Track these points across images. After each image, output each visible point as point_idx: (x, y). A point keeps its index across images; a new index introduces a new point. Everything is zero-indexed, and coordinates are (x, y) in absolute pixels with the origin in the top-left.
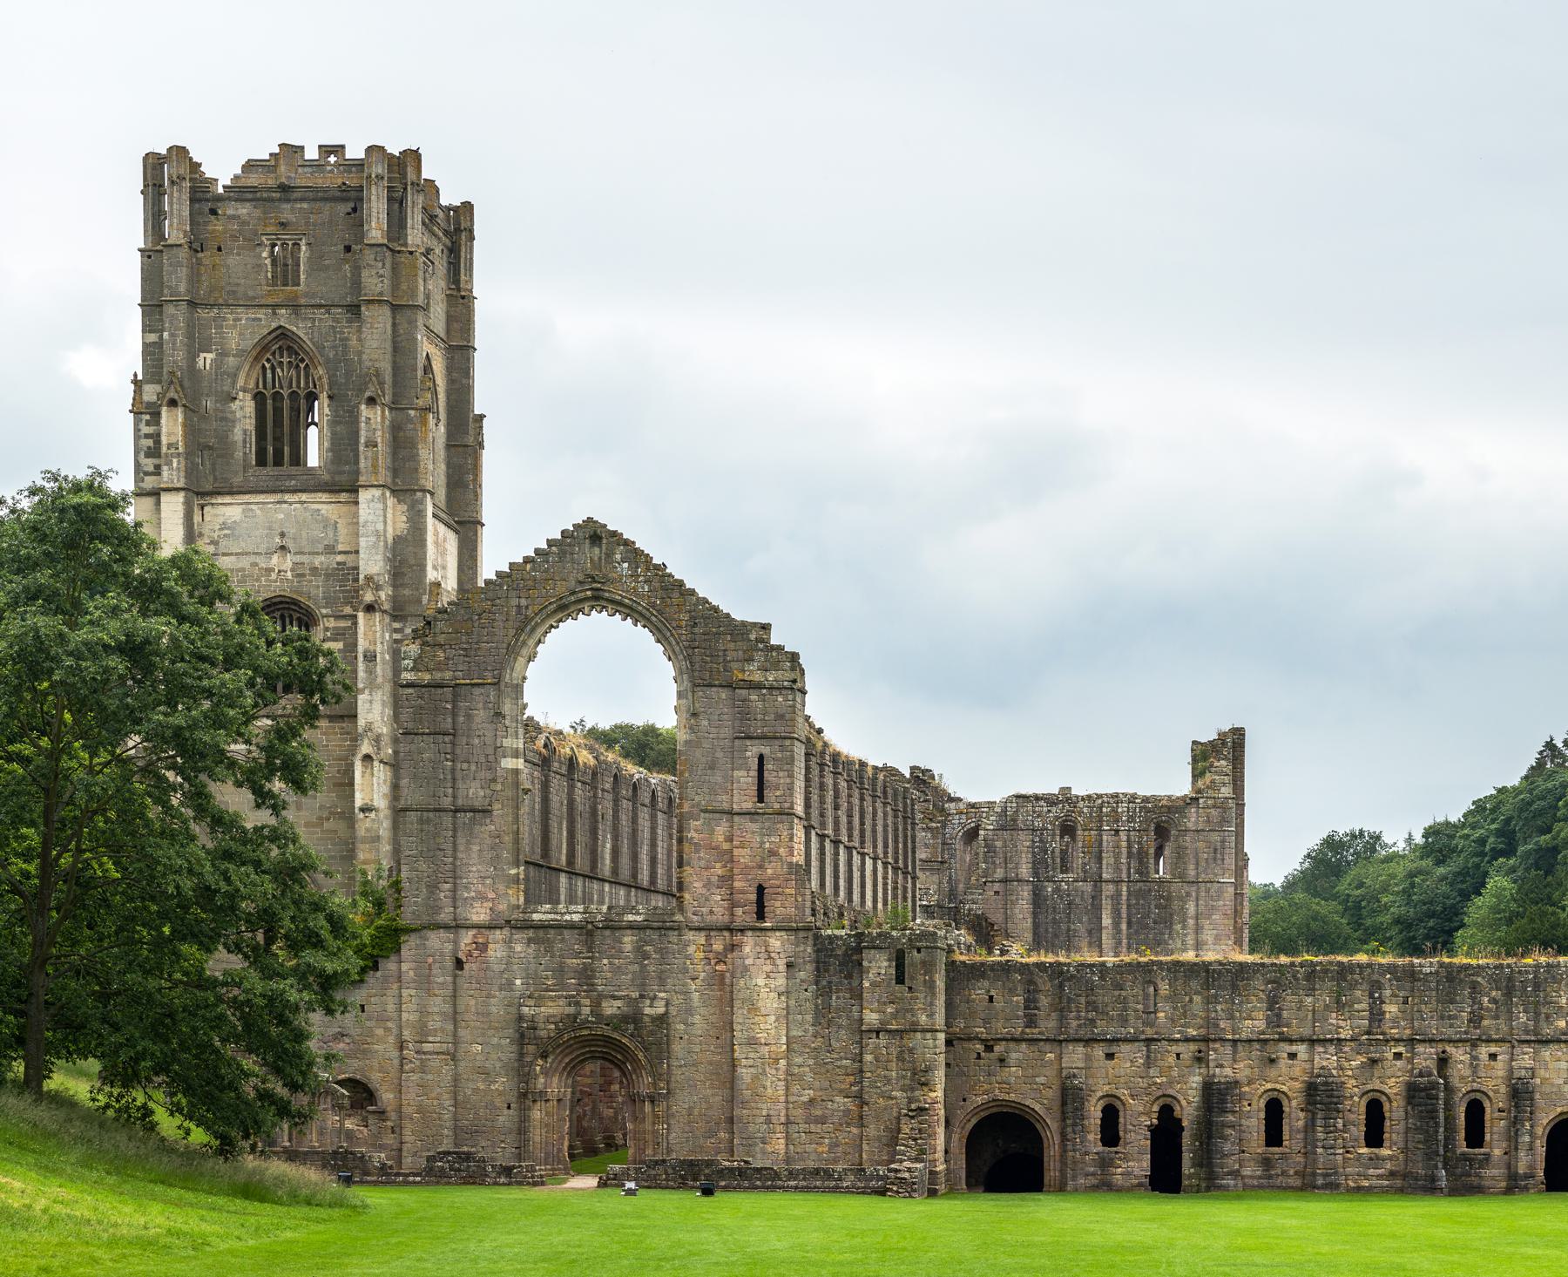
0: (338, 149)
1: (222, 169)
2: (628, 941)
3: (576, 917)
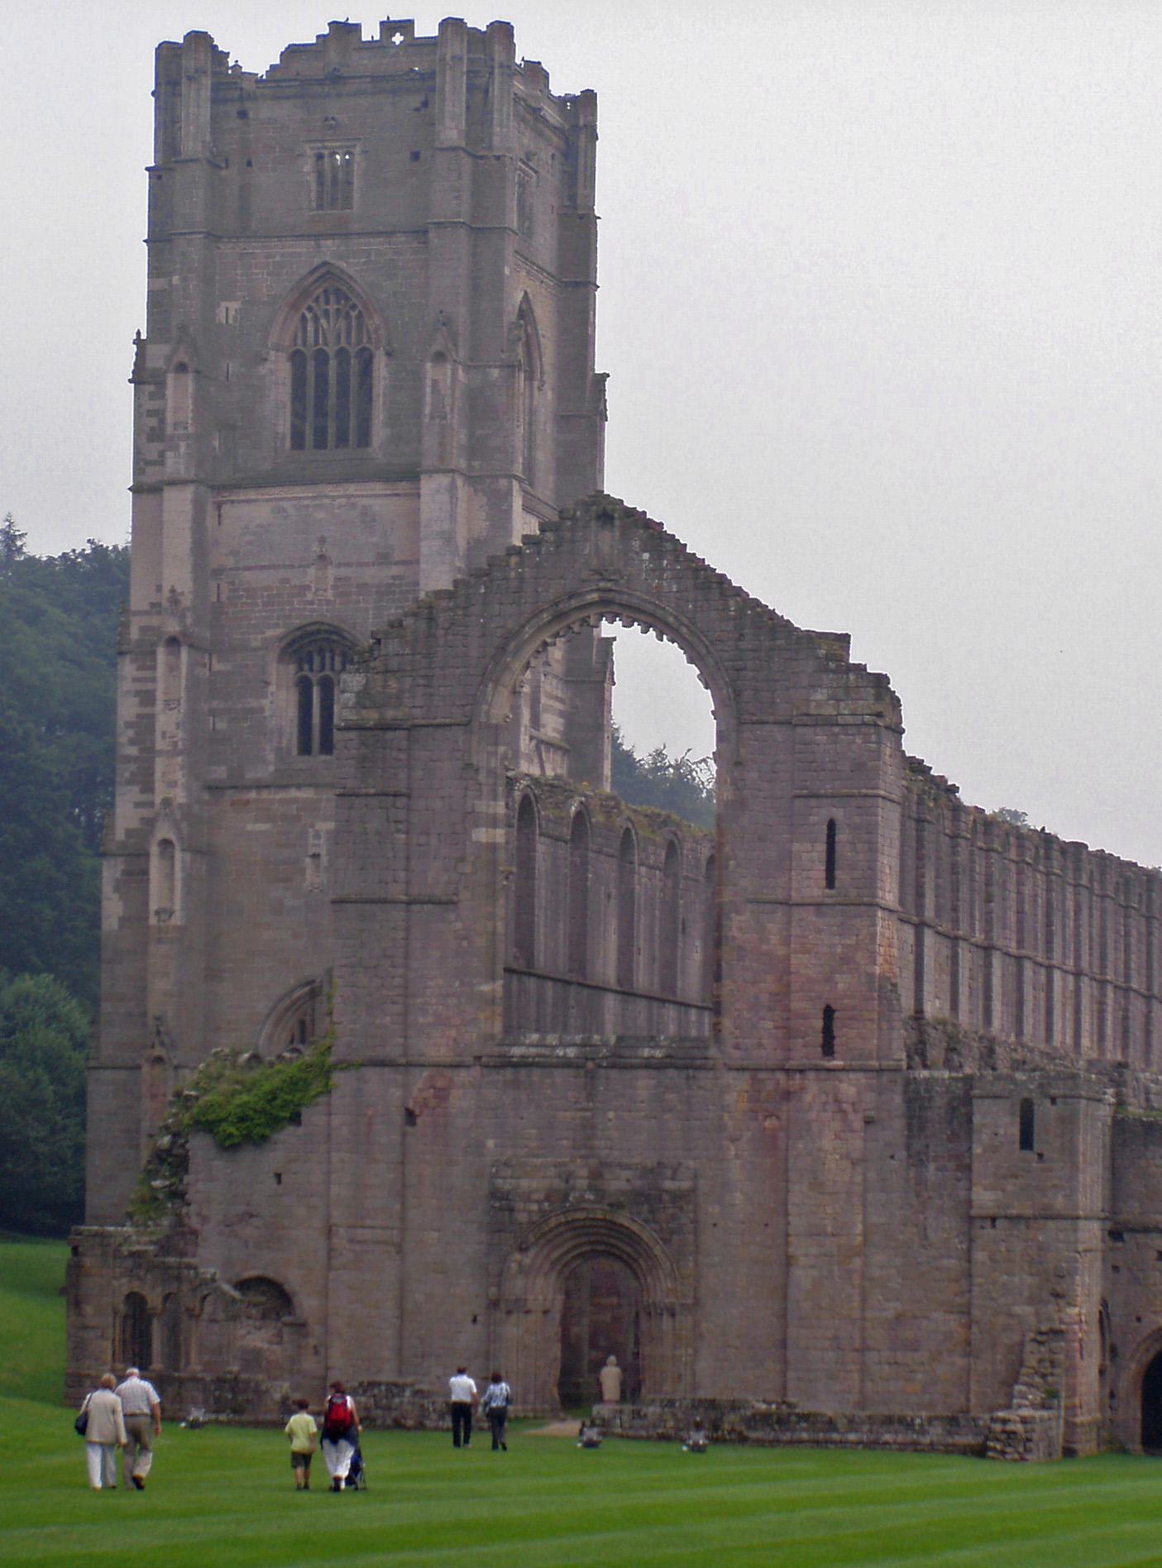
0: (406, 26)
1: (254, 53)
2: (644, 1083)
3: (571, 1052)
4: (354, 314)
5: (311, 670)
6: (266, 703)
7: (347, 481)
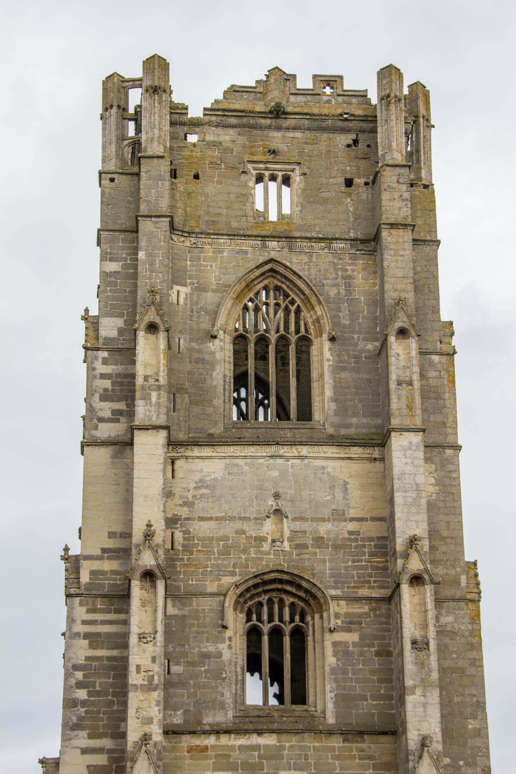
0: (333, 81)
4: (293, 308)
5: (259, 619)
6: (223, 647)
7: (301, 443)
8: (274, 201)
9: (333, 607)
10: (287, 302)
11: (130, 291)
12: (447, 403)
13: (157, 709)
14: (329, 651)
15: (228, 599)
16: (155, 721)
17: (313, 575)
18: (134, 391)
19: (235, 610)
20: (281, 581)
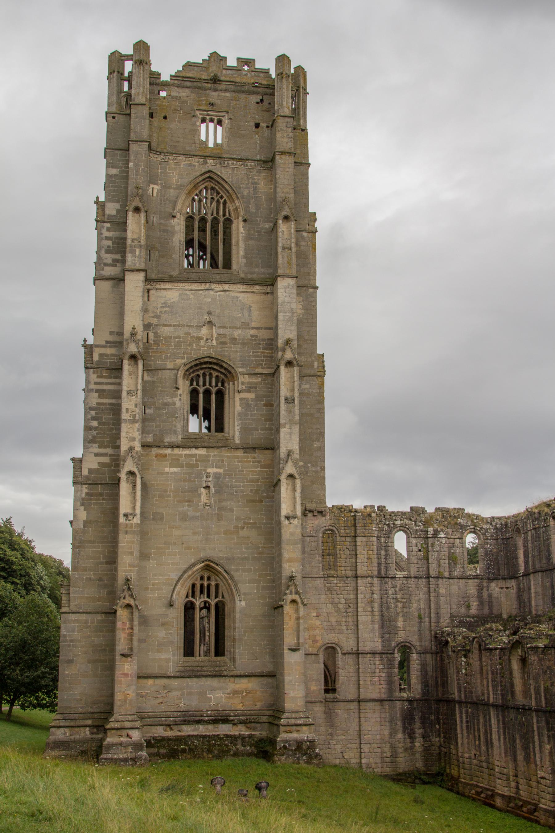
0: (249, 62)
4: (222, 201)
6: (176, 400)
7: (225, 283)
8: (212, 135)
9: (241, 378)
10: (218, 197)
11: (124, 187)
12: (311, 261)
13: (138, 433)
14: (238, 403)
15: (179, 373)
16: (137, 440)
17: (230, 360)
18: (126, 248)
19: (184, 379)
20: (211, 363)
